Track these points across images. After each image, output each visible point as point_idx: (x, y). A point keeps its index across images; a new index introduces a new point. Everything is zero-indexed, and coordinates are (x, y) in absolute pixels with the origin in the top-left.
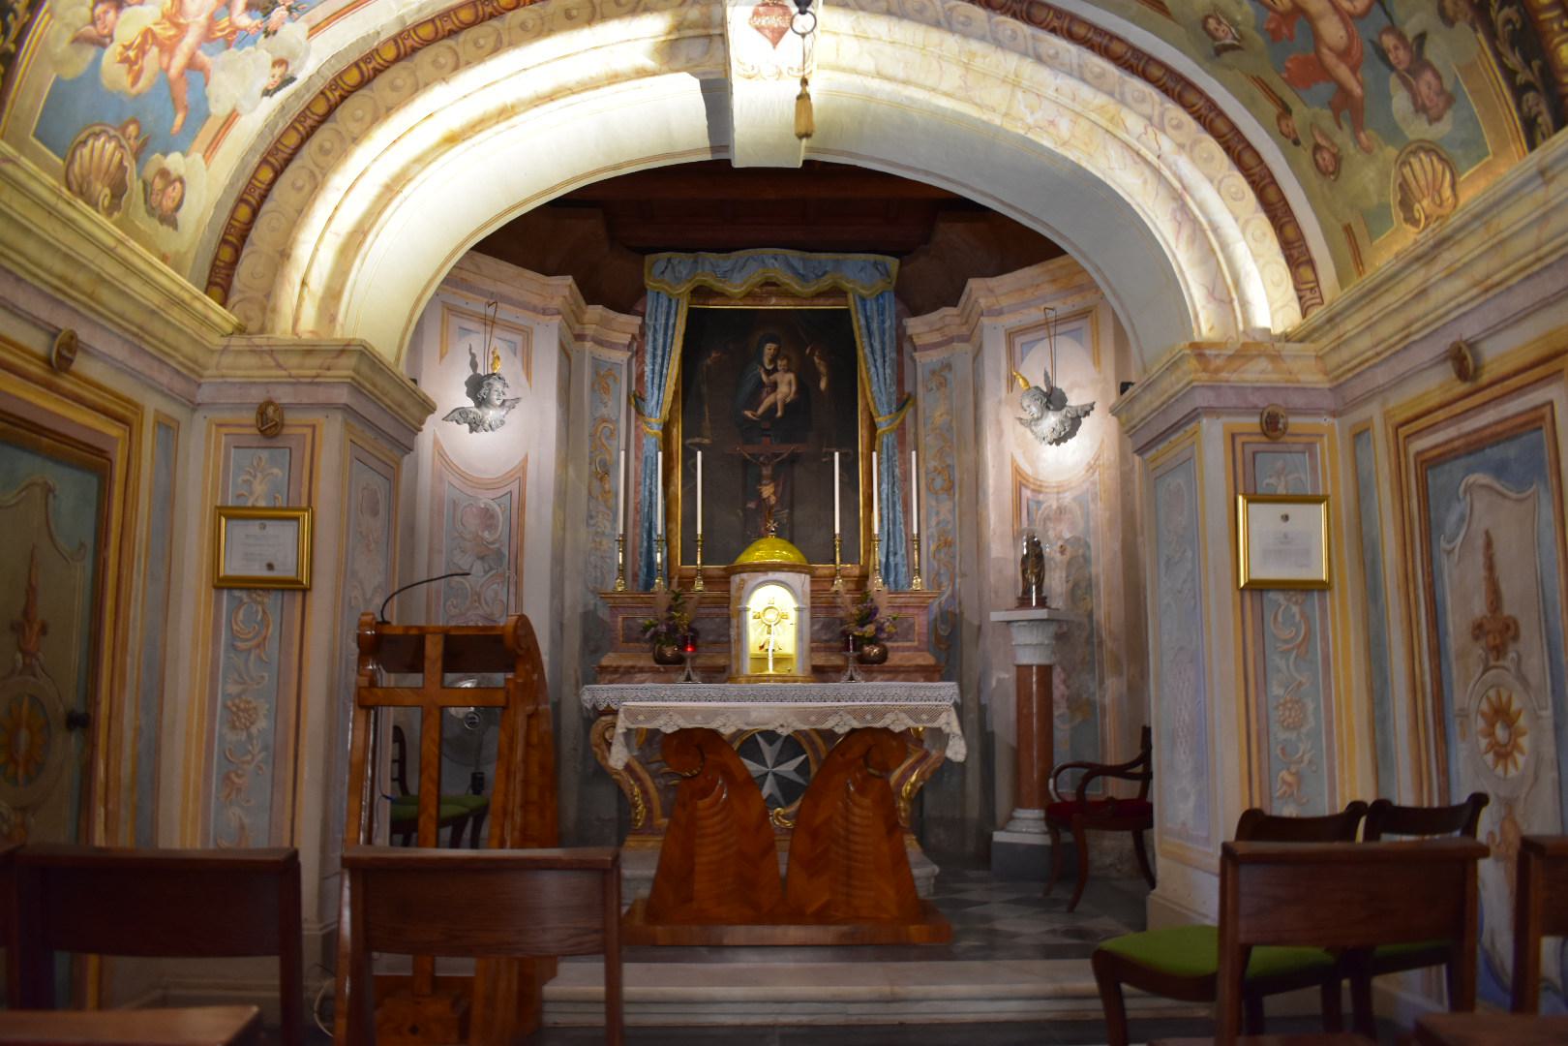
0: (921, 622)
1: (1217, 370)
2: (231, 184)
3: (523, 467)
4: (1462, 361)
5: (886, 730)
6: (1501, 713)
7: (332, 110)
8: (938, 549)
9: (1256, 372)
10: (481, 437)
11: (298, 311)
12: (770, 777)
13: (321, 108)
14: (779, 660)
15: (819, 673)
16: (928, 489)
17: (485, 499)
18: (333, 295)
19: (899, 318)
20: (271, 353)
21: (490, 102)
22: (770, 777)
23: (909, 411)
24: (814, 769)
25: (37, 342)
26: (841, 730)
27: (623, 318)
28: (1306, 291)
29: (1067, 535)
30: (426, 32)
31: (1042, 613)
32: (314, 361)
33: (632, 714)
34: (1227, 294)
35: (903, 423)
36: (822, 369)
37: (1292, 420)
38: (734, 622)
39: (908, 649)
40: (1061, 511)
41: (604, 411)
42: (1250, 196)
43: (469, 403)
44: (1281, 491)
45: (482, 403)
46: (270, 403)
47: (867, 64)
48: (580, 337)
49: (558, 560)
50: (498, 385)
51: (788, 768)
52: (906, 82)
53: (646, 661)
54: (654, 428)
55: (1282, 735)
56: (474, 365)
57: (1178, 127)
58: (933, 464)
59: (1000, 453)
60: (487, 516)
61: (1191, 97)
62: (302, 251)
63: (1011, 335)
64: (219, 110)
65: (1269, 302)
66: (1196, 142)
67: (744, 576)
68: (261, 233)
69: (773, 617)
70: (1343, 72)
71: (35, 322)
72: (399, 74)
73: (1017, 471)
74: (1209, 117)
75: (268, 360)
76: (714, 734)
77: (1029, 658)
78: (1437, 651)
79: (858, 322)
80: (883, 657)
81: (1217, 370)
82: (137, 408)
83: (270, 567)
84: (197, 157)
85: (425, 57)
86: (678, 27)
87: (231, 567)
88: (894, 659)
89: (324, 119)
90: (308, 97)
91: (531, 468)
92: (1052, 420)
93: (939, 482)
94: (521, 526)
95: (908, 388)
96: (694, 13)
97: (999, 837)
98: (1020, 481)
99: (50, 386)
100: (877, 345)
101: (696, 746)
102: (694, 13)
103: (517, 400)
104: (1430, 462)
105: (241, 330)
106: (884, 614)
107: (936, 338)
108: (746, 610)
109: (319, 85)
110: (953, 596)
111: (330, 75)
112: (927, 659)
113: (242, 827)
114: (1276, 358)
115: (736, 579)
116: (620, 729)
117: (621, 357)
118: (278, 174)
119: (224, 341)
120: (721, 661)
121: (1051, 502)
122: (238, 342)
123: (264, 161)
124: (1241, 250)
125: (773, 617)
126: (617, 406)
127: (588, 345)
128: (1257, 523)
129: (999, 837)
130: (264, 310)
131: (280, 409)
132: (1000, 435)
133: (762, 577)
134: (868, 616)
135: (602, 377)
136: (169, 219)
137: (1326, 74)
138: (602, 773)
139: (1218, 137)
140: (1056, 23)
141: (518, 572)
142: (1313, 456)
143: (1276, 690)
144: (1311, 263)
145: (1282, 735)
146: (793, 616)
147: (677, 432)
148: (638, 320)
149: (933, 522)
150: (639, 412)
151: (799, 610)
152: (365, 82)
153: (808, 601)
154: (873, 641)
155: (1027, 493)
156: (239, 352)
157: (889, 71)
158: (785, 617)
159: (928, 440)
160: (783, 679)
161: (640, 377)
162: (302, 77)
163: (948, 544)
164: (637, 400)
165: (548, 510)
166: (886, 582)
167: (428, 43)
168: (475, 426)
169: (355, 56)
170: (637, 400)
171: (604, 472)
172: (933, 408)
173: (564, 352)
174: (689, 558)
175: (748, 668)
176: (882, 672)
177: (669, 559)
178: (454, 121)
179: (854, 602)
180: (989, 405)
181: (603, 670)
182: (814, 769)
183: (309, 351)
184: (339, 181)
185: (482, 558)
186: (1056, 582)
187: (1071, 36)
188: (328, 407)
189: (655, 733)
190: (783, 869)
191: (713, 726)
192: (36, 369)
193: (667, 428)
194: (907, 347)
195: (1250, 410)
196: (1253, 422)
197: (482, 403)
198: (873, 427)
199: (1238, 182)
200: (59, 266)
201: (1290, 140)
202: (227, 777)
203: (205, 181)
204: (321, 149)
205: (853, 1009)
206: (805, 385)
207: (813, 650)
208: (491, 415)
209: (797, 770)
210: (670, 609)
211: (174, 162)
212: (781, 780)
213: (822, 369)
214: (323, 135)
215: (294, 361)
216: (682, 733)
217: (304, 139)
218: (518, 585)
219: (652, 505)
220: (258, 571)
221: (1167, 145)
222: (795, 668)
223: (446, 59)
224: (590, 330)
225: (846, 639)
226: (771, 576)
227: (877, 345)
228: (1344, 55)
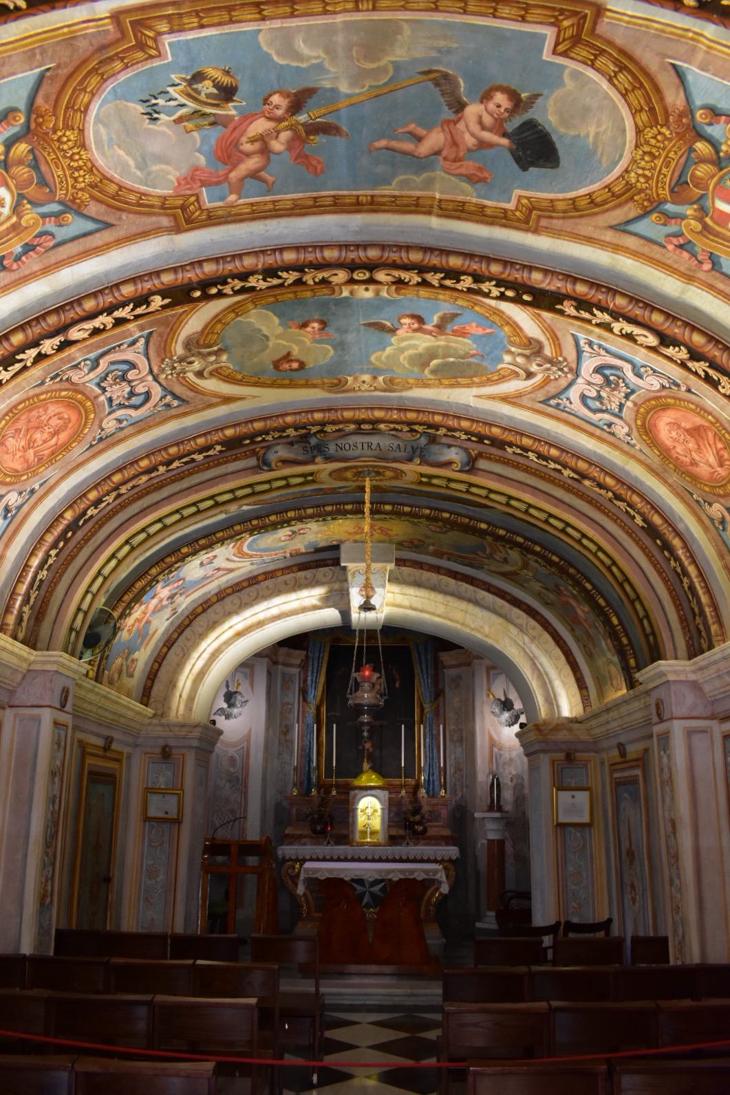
0: (444, 812)
1: (546, 735)
2: (152, 654)
3: (249, 735)
4: (621, 747)
5: (414, 879)
6: (633, 887)
7: (191, 622)
8: (455, 772)
9: (562, 736)
10: (232, 721)
11: (178, 707)
12: (367, 895)
13: (187, 622)
14: (373, 833)
15: (393, 840)
16: (450, 740)
17: (231, 752)
18: (191, 698)
20: (168, 726)
21: (254, 619)
22: (367, 895)
23: (441, 699)
24: (389, 889)
25: (100, 742)
26: (396, 879)
27: (297, 652)
28: (585, 700)
29: (514, 773)
30: (229, 591)
31: (497, 815)
32: (186, 729)
33: (307, 870)
34: (551, 700)
35: (438, 705)
36: (397, 677)
37: (577, 754)
38: (351, 814)
39: (438, 826)
40: (511, 760)
41: (287, 700)
42: (563, 658)
43: (225, 706)
44: (573, 785)
45: (231, 705)
46: (167, 746)
47: (406, 603)
48: (276, 663)
49: (264, 779)
50: (239, 697)
51: (376, 889)
52: (422, 611)
53: (307, 831)
54: (312, 710)
55: (573, 887)
56: (227, 686)
57: (533, 629)
58: (453, 727)
59: (483, 726)
60: (232, 760)
61: (539, 618)
62: (180, 684)
64: (151, 632)
65: (568, 705)
66: (541, 635)
67: (356, 791)
68: (163, 674)
69: (370, 811)
70: (586, 626)
71: (97, 735)
72: (218, 607)
73: (491, 738)
74: (546, 625)
75: (167, 729)
76: (342, 880)
77: (492, 836)
78: (620, 858)
79: (415, 655)
80: (425, 831)
81: (546, 735)
82: (121, 753)
83: (167, 813)
84: (142, 650)
85: (228, 600)
86: (330, 591)
87: (152, 812)
88: (431, 832)
89: (188, 626)
90: (182, 619)
91: (253, 738)
92: (506, 715)
93: (455, 737)
94: (248, 764)
95: (441, 686)
96: (336, 586)
97: (478, 925)
98: (493, 744)
99: (104, 757)
100: (424, 667)
101: (333, 887)
102: (336, 586)
103: (246, 701)
104: (618, 784)
105: (155, 715)
106: (425, 808)
107: (454, 662)
108: (357, 809)
109: (187, 613)
110: (462, 796)
111: (191, 609)
112: (446, 832)
113: (152, 920)
114: (570, 730)
115: (352, 793)
116: (302, 878)
117: (295, 671)
118: (169, 649)
119: (149, 721)
120: (344, 832)
121: (506, 756)
122: (155, 721)
123: (164, 645)
124: (558, 685)
125: (370, 811)
126: (294, 697)
127: (280, 667)
128: (565, 796)
129: (478, 925)
130: (163, 705)
131: (170, 747)
132: (483, 719)
133: (365, 793)
134: (417, 810)
135: (287, 681)
136: (131, 676)
137: (580, 623)
138: (293, 897)
139: (551, 634)
141: (246, 787)
142: (587, 770)
143: (570, 869)
144: (586, 688)
145: (573, 887)
146: (380, 811)
147: (324, 709)
148: (304, 653)
149: (453, 758)
150: (305, 700)
151: (382, 809)
152: (204, 611)
153: (387, 804)
154: (419, 823)
155: (495, 750)
156: (155, 725)
157: (415, 605)
158: (375, 811)
159: (451, 715)
160: (375, 845)
161: (305, 681)
162: (180, 611)
163: (461, 770)
164: (304, 692)
165: (260, 756)
166: (428, 792)
167: (229, 595)
168: (228, 717)
169: (201, 601)
170: (304, 692)
171: (287, 730)
172: (453, 699)
173: (269, 673)
174: (329, 775)
175: (358, 838)
176: (424, 839)
177: (319, 777)
178: (240, 627)
179: (411, 802)
180: (478, 704)
181: (287, 836)
182: (389, 889)
183: (183, 726)
184: (195, 655)
185: (229, 781)
186: (508, 795)
187: (489, 591)
188: (190, 747)
189: (317, 879)
190: (371, 940)
191: (341, 877)
192: (101, 753)
193: (318, 709)
195: (561, 751)
196: (562, 755)
197: (231, 705)
198: (422, 709)
199: (558, 652)
200: (111, 716)
201: (577, 640)
202: (147, 899)
203: (143, 656)
204: (188, 639)
205: (396, 999)
207: (389, 826)
208: (235, 711)
209: (380, 890)
210: (320, 806)
211: (136, 655)
212: (372, 894)
213: (397, 677)
214: (188, 632)
215: (177, 729)
216: (328, 879)
217: (180, 635)
218: (246, 793)
219: (310, 749)
220: (161, 815)
221: (526, 639)
222: (380, 838)
223: (237, 601)
224: (281, 659)
225: (406, 822)
226: (369, 792)
227: (424, 667)
228: (586, 621)
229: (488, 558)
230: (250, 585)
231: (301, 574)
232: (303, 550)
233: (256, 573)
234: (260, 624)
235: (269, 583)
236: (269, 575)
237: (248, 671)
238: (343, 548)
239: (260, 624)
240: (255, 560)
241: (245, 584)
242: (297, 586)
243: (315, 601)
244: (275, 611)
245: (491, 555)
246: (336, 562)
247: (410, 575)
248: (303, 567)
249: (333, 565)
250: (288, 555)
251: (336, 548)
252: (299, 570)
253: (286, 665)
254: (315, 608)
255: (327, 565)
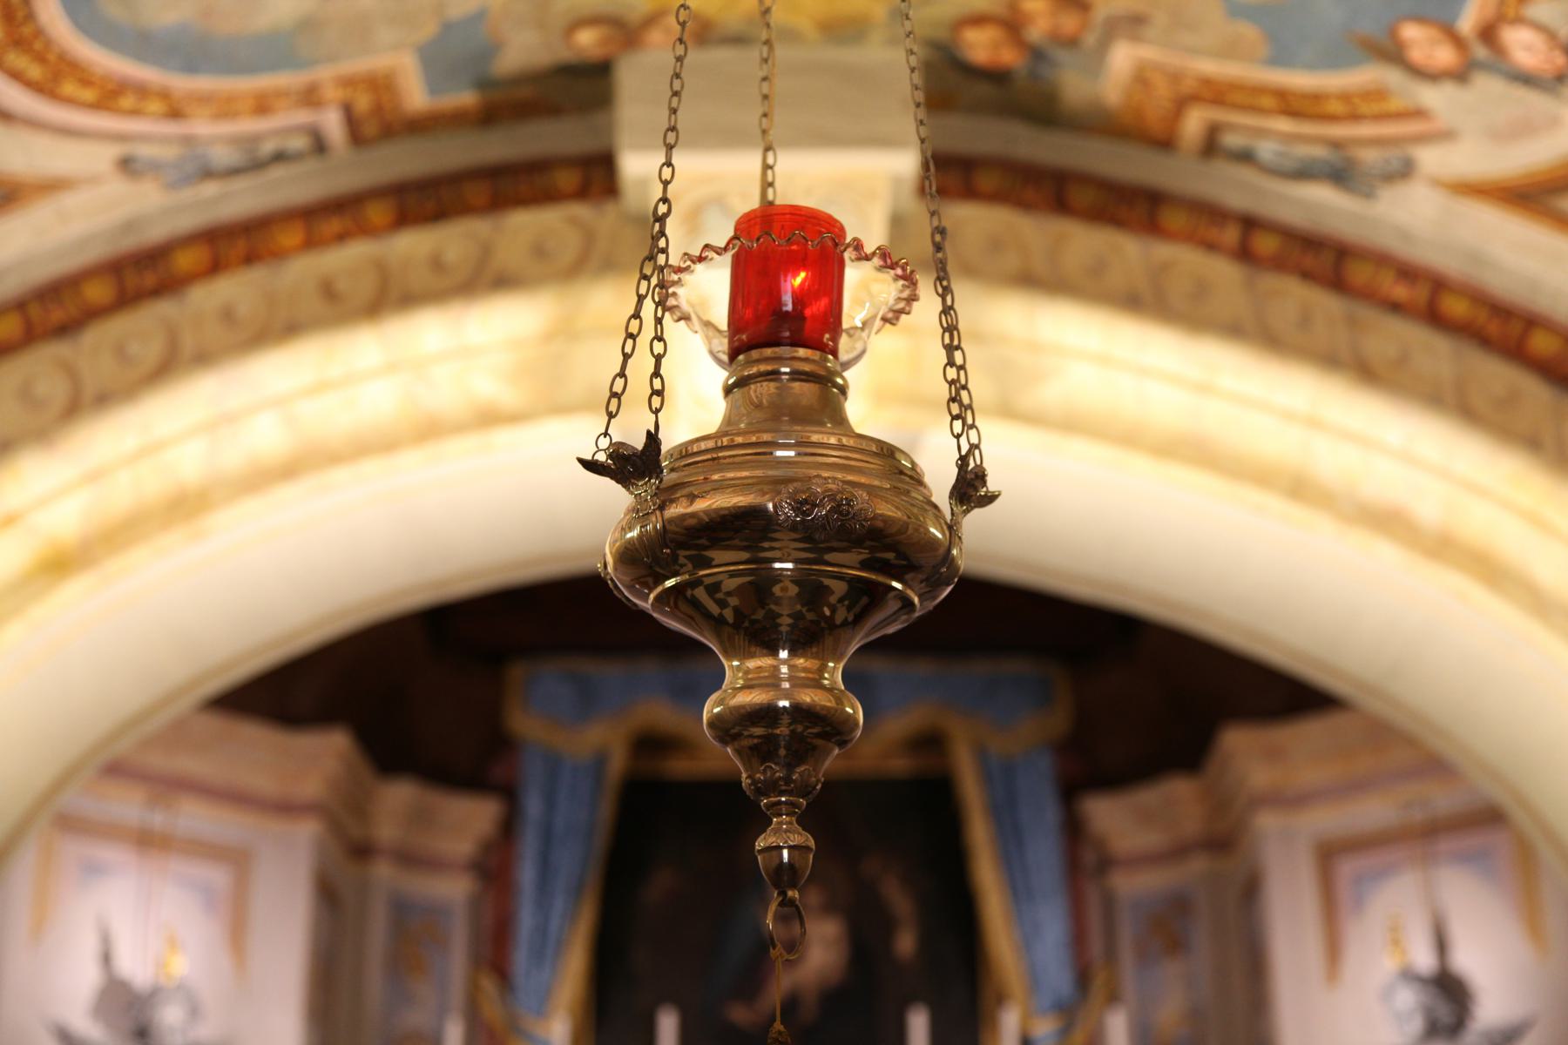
19: (1071, 790)
48: (362, 851)
63: (1329, 854)
140: (1401, 292)
194: (1089, 858)
206: (866, 946)
229: (1460, 75)
230: (126, 300)
231: (413, 244)
232: (416, 96)
233: (156, 233)
234: (185, 507)
235: (235, 289)
236: (235, 244)
237: (218, 876)
238: (638, 84)
239: (185, 507)
240: (152, 134)
241: (97, 292)
242: (388, 298)
243: (488, 384)
244: (265, 437)
245: (1488, 34)
246: (597, 175)
247: (996, 245)
248: (423, 201)
249: (582, 193)
250: (332, 123)
251: (583, 85)
252: (404, 219)
253: (409, 859)
254: (489, 418)
255: (548, 197)
